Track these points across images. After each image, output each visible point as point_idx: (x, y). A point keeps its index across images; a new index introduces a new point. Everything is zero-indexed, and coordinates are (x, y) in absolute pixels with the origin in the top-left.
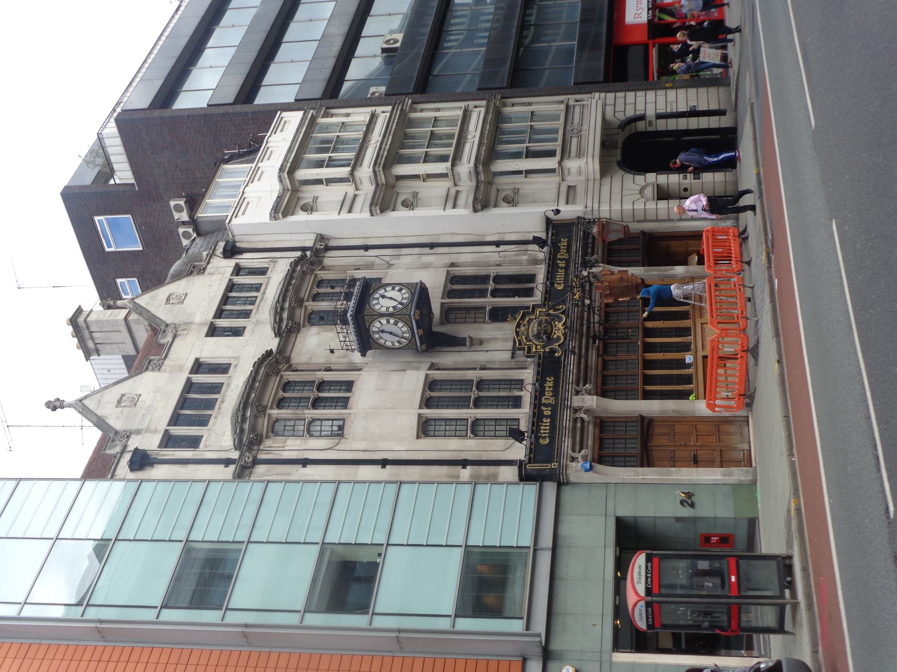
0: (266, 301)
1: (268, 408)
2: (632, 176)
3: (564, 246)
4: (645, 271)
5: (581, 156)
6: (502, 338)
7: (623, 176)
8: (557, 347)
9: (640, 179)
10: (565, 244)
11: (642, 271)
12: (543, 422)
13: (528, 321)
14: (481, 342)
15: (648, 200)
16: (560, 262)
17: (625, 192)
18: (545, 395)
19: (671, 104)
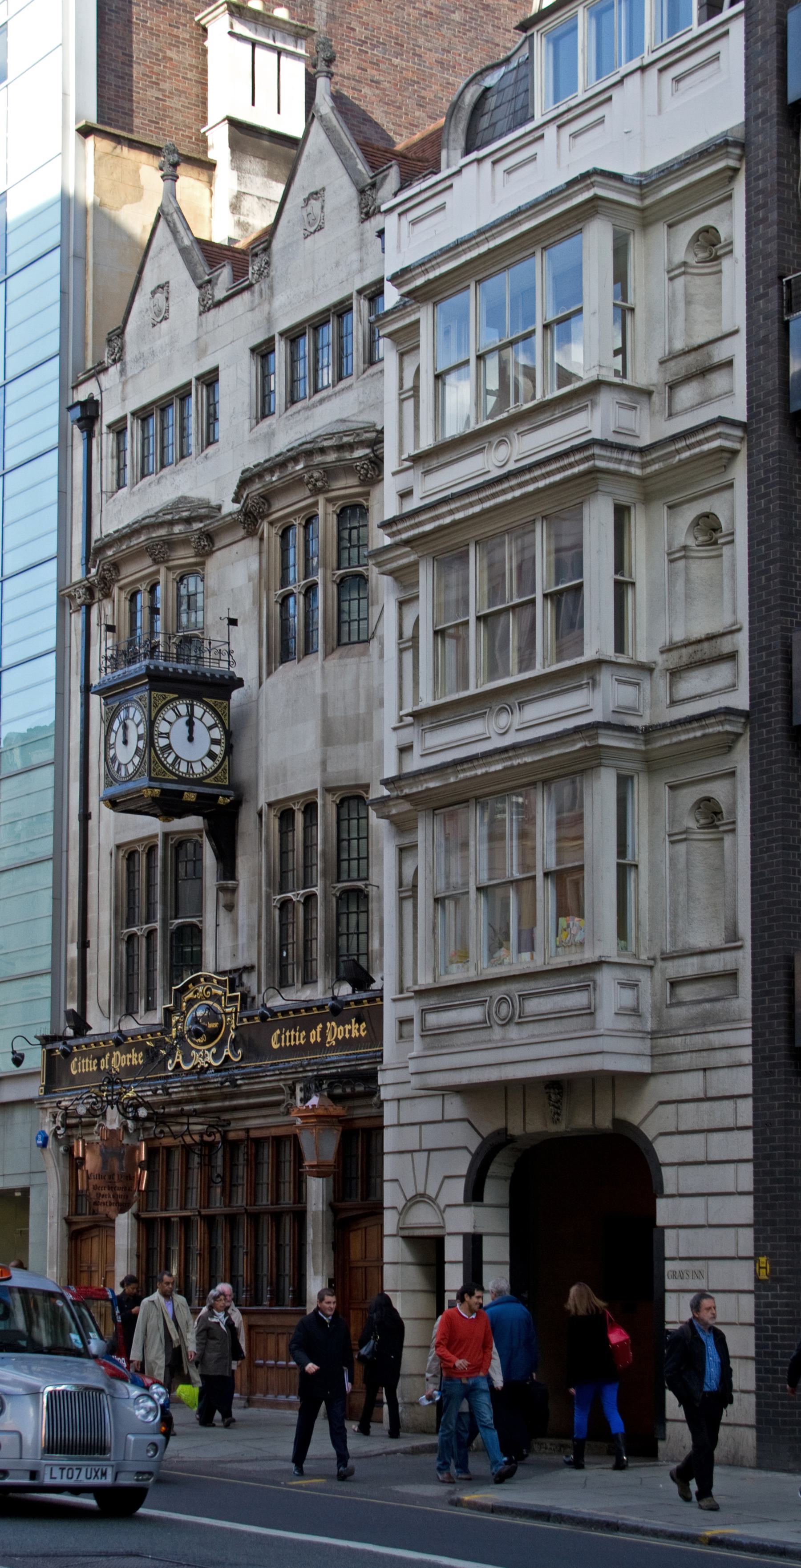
0: (307, 418)
1: (167, 565)
2: (464, 1170)
3: (350, 1032)
4: (315, 1213)
5: (428, 1039)
6: (237, 945)
7: (466, 1148)
8: (176, 1060)
9: (456, 1191)
10: (355, 1034)
11: (314, 1208)
12: (300, 1032)
13: (216, 995)
14: (230, 907)
15: (400, 1214)
16: (319, 1030)
17: (421, 1158)
18: (338, 1027)
19: (698, 1275)
